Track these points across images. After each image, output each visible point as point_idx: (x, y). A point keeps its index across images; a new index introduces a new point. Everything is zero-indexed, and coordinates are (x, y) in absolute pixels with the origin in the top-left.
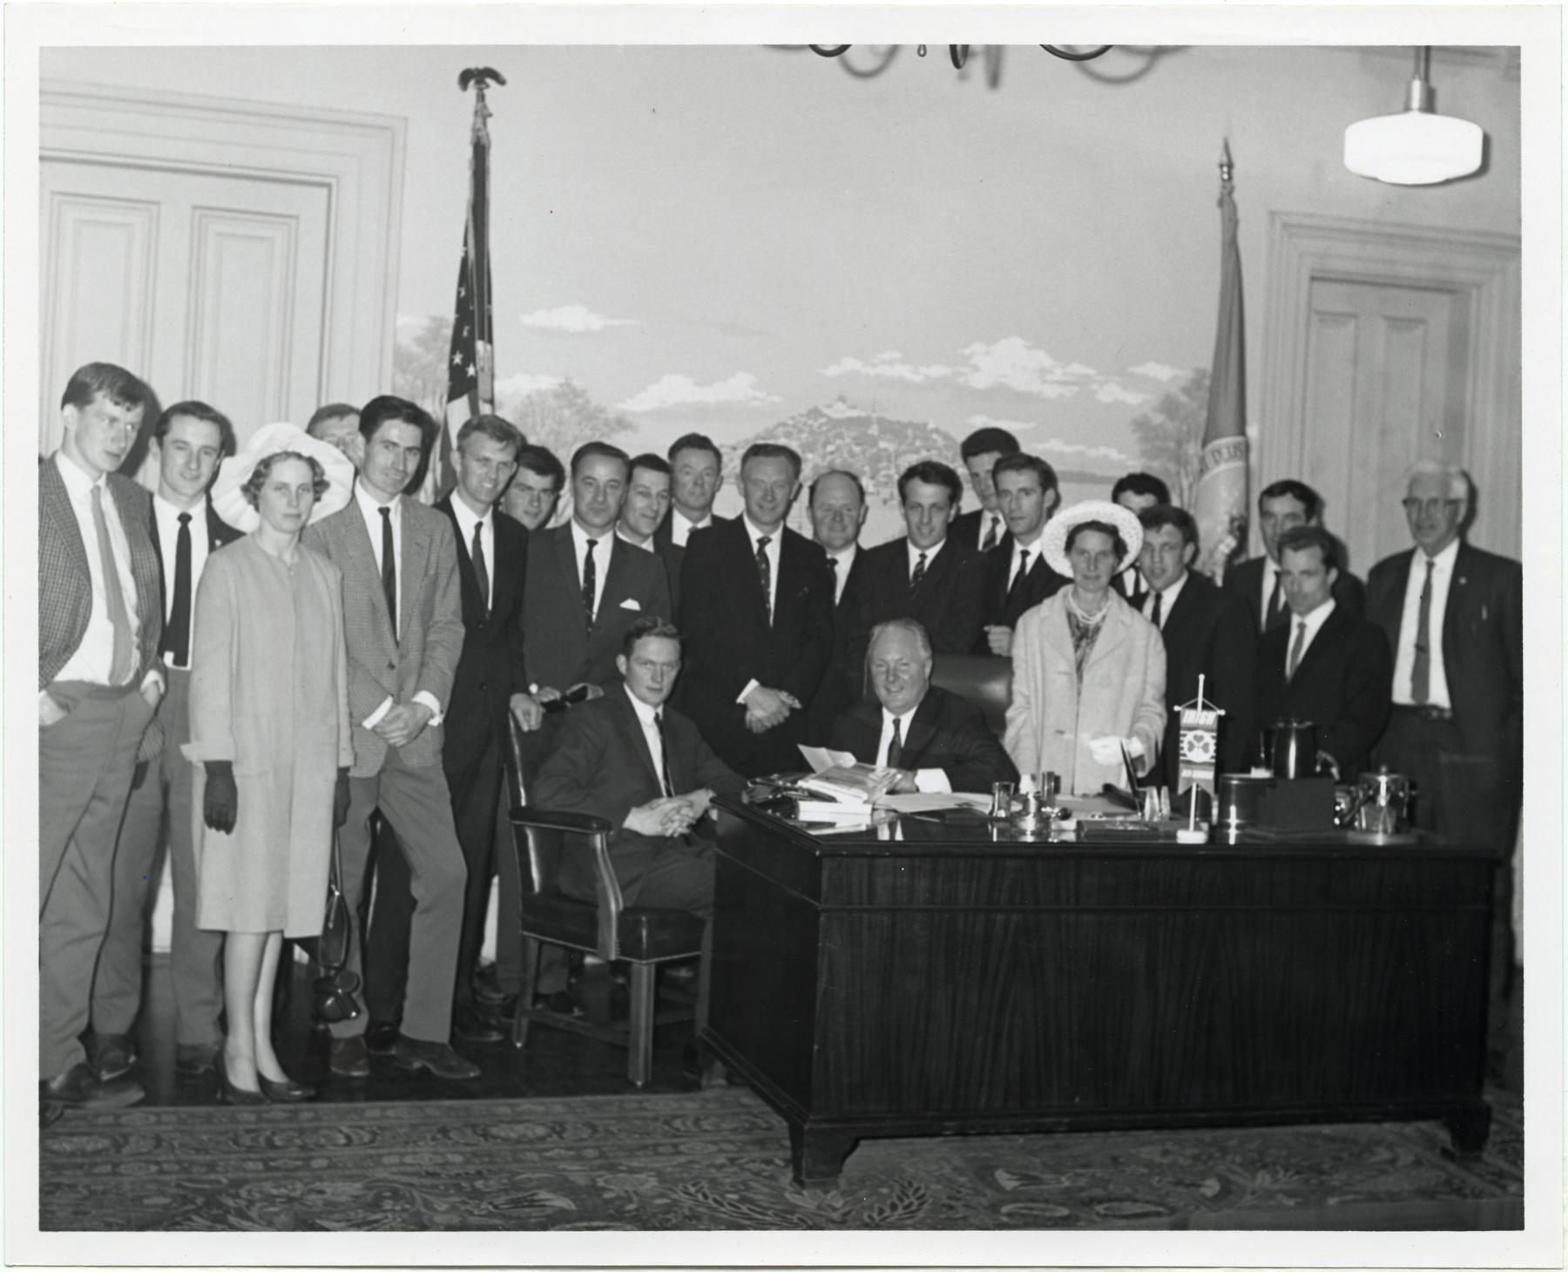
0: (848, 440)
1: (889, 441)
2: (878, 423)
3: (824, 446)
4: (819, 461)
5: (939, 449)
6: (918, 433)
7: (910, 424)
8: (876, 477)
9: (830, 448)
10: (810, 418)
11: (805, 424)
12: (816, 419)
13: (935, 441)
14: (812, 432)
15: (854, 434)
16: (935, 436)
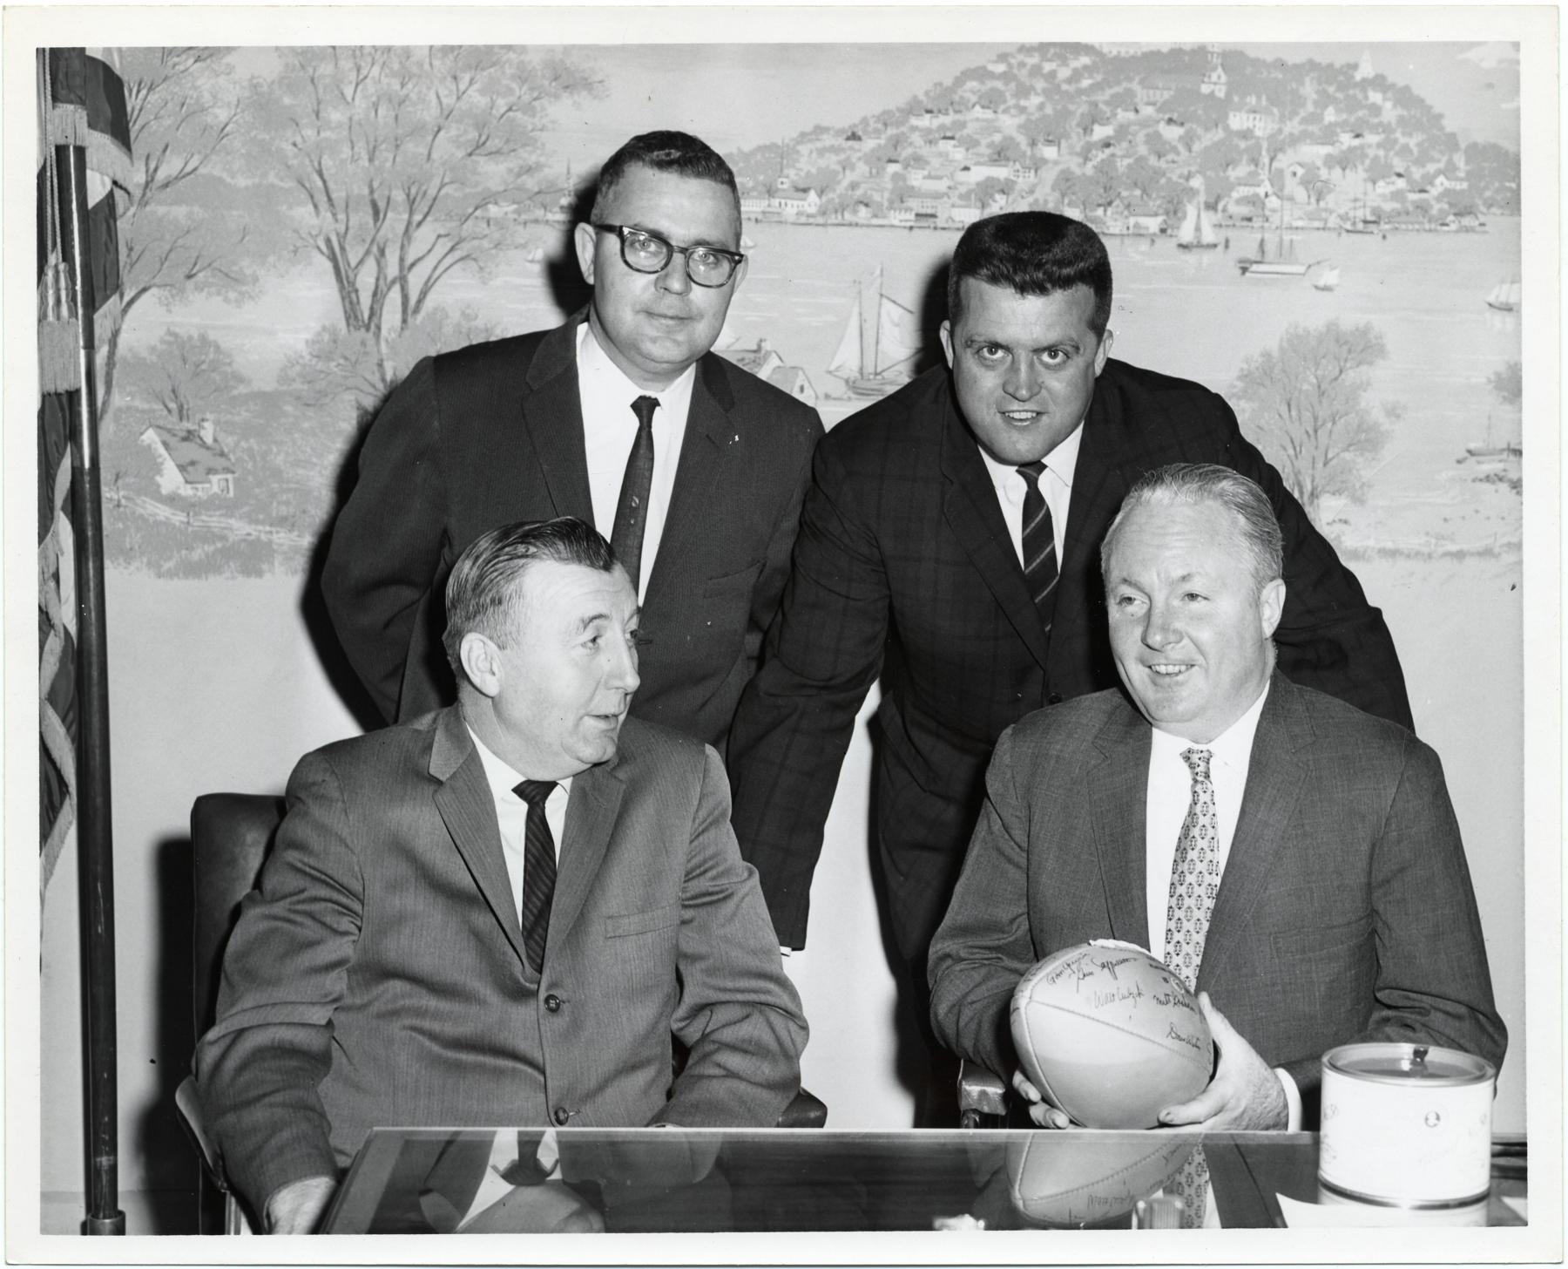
0: (1148, 111)
1: (1255, 112)
2: (1224, 69)
3: (1087, 130)
4: (1074, 164)
5: (1387, 129)
6: (1331, 89)
7: (1312, 65)
8: (1220, 207)
9: (1100, 132)
10: (1045, 59)
11: (1036, 71)
12: (1064, 61)
13: (1376, 110)
14: (1053, 90)
15: (1164, 96)
16: (1375, 97)
